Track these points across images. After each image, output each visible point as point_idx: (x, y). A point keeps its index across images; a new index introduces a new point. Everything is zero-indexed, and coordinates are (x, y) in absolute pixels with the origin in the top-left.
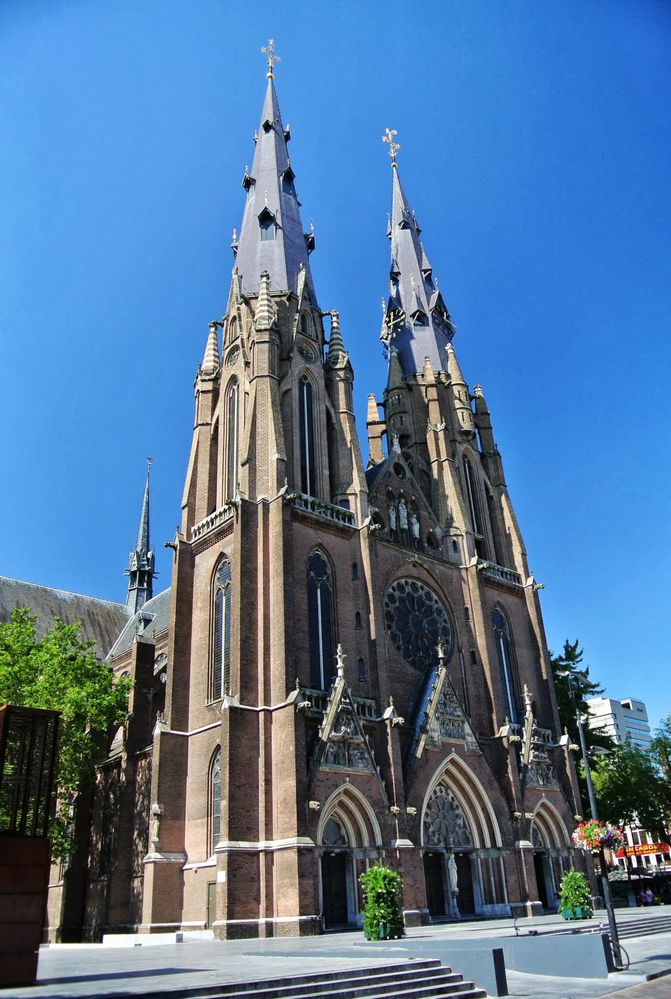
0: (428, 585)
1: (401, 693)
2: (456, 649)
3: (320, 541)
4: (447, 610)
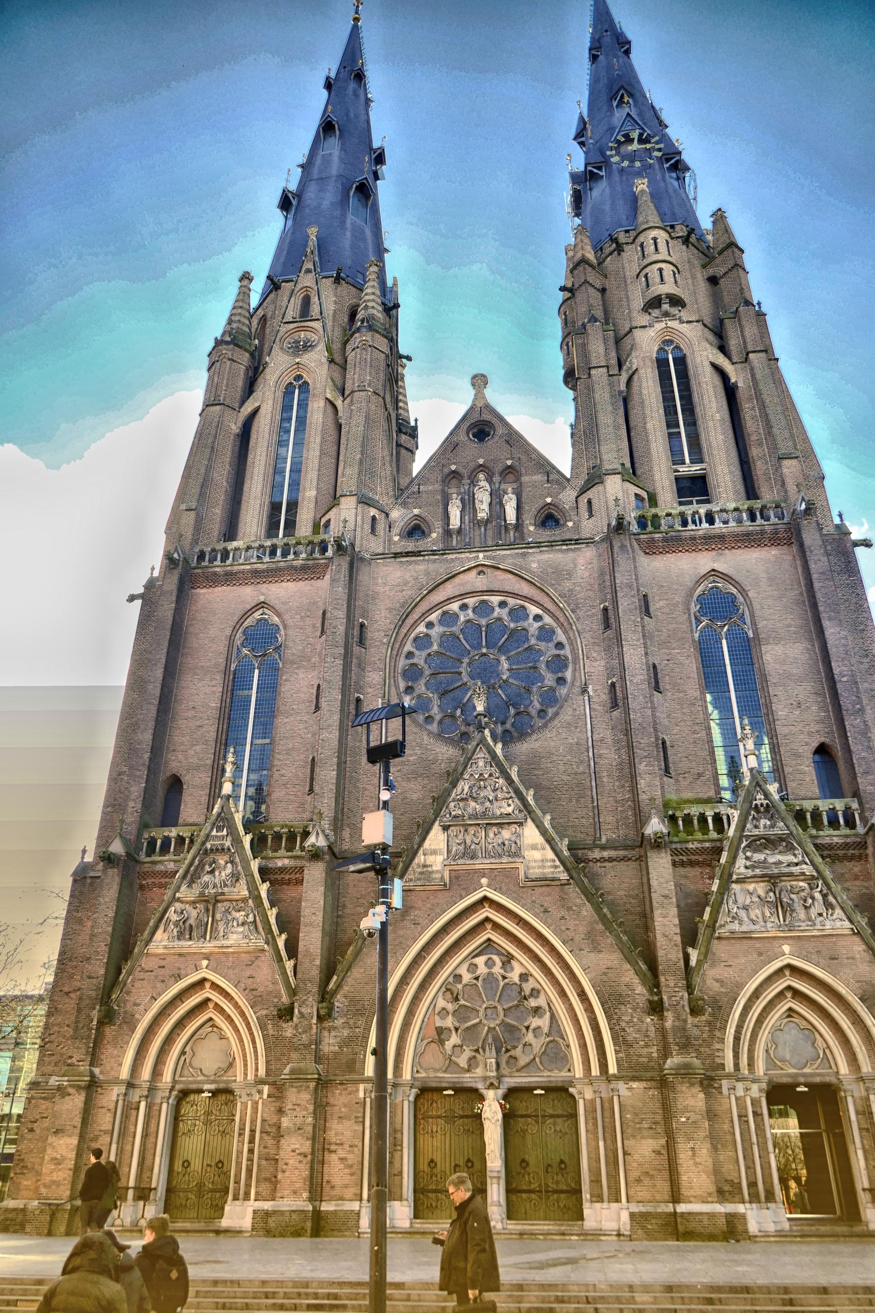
0: (515, 595)
1: (415, 796)
2: (577, 690)
3: (262, 598)
4: (561, 625)
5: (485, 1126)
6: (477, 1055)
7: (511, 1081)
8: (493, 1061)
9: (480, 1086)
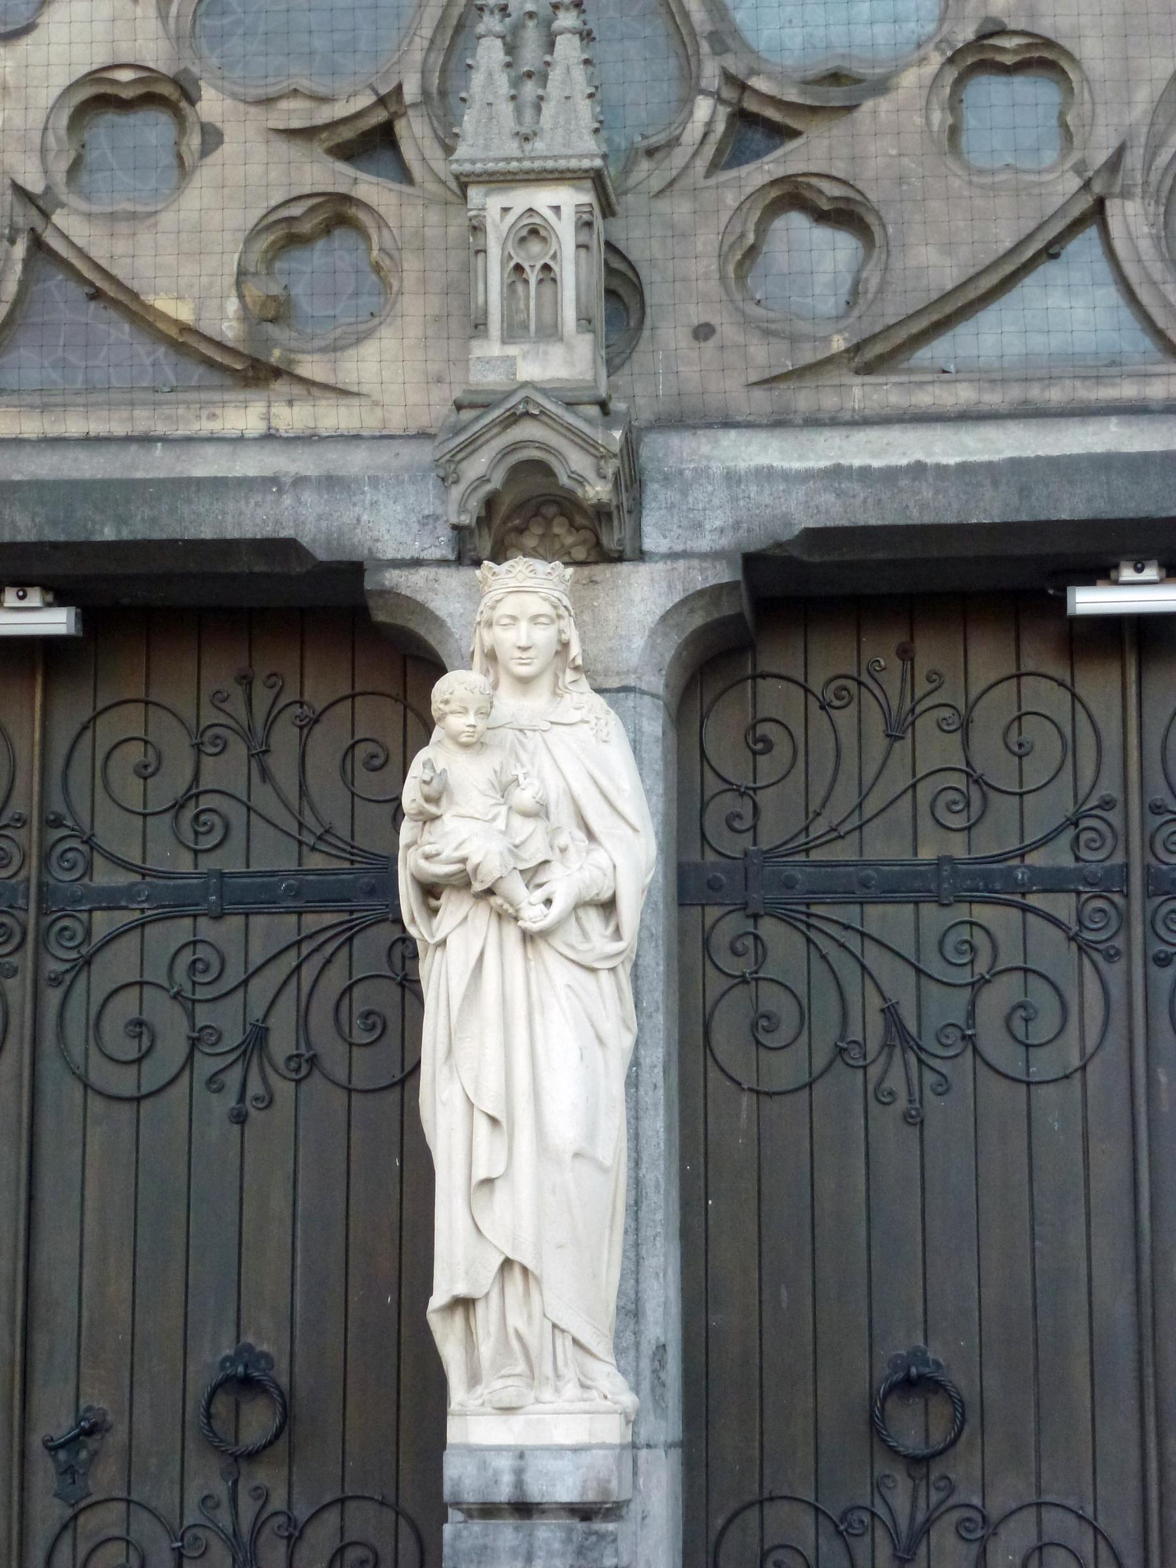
5: (442, 978)
6: (371, 188)
7: (760, 475)
8: (560, 205)
9: (392, 526)
